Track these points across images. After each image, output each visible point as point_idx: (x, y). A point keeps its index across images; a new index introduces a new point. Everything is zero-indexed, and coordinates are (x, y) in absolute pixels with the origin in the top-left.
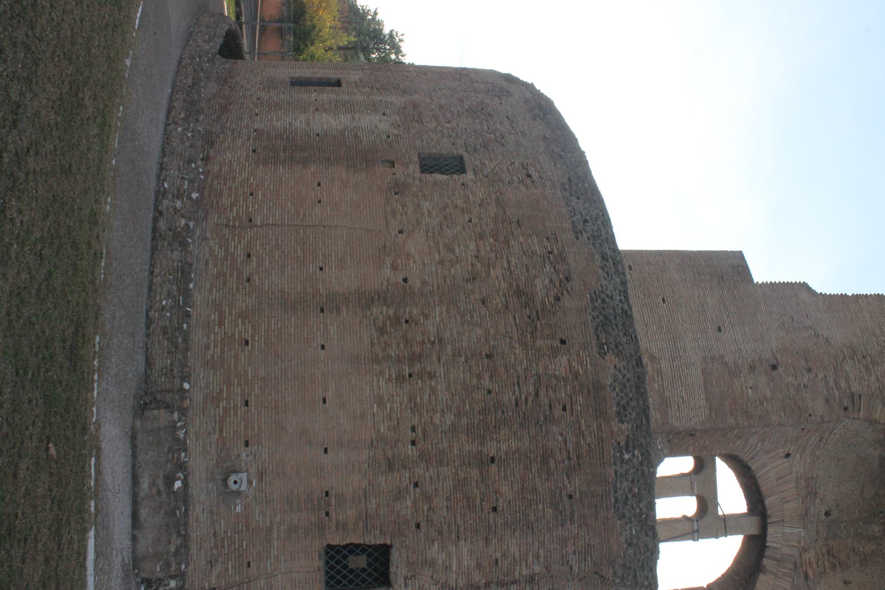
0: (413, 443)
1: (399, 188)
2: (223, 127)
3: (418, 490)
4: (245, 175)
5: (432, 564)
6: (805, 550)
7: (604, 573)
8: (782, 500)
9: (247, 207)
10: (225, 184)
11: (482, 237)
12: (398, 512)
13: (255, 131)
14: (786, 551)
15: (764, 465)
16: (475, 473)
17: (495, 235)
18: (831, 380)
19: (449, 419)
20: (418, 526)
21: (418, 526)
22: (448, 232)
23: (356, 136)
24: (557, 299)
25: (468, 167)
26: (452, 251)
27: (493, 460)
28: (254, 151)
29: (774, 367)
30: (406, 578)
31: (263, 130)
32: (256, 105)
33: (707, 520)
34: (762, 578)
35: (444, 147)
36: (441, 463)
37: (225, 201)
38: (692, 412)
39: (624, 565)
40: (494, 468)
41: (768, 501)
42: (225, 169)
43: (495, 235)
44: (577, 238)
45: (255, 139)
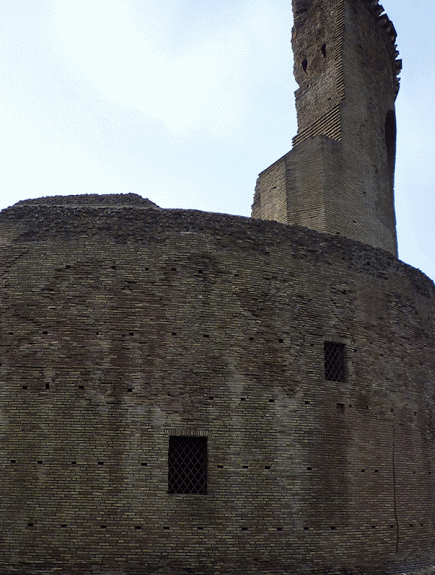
1: (363, 404)
2: (304, 561)
4: (358, 534)
9: (384, 529)
10: (367, 551)
11: (392, 351)
13: (306, 529)
17: (390, 341)
18: (378, 137)
22: (391, 375)
23: (310, 432)
24: (416, 313)
25: (338, 340)
26: (400, 375)
28: (333, 528)
29: (376, 172)
31: (305, 521)
32: (260, 531)
35: (317, 353)
37: (380, 548)
42: (354, 552)
43: (390, 341)
44: (386, 279)
45: (318, 527)
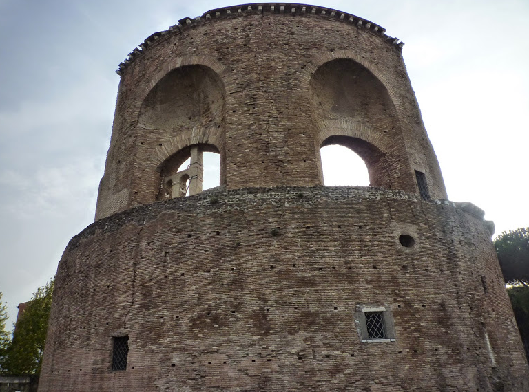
0: (85, 328)
3: (98, 324)
5: (121, 315)
6: (202, 125)
7: (139, 230)
8: (179, 142)
12: (102, 334)
14: (201, 133)
15: (164, 154)
16: (97, 297)
19: (82, 312)
20: (107, 323)
21: (107, 323)
27: (94, 290)
30: (125, 328)
33: (189, 174)
34: (210, 142)
36: (91, 314)
38: (125, 194)
39: (139, 221)
40: (97, 289)
41: (180, 148)
